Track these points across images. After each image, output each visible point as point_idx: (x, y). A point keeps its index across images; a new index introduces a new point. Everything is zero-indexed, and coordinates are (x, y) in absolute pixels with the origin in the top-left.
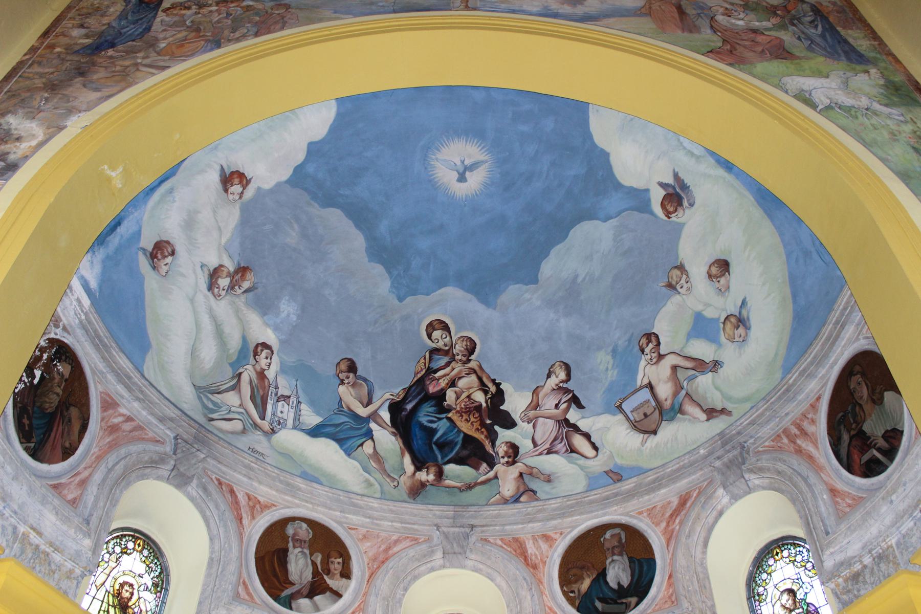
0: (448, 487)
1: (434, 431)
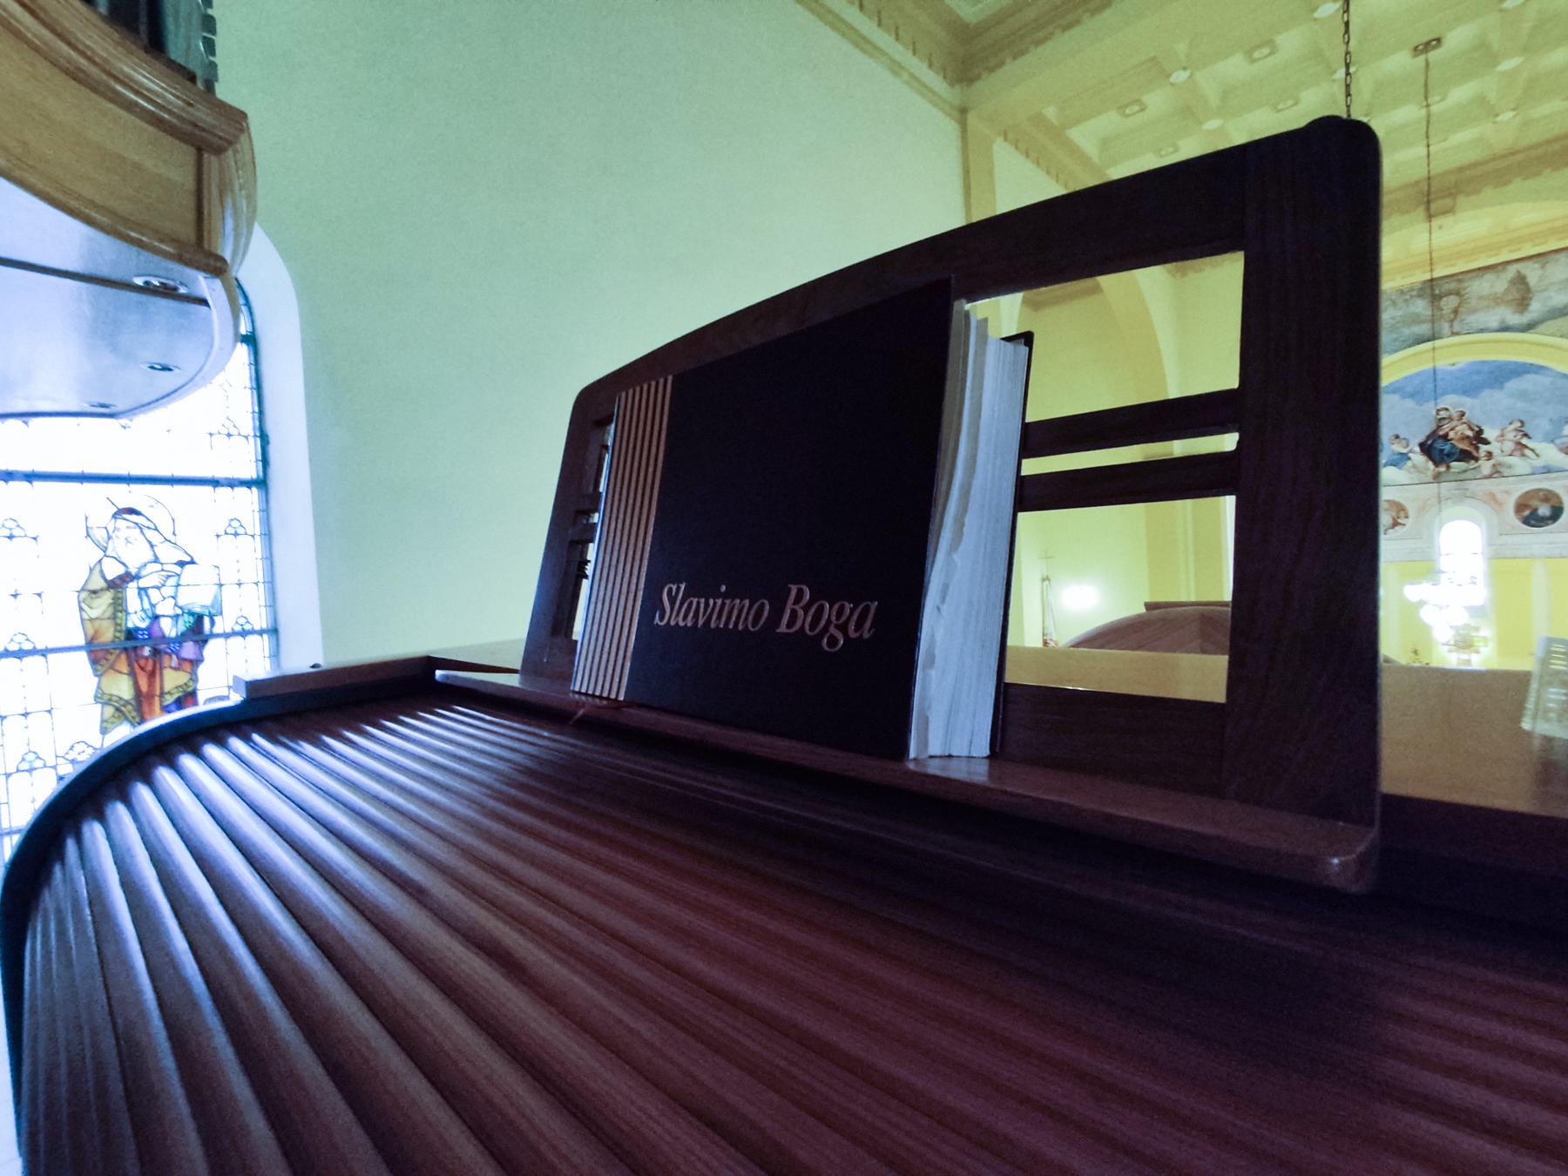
0: (1454, 472)
1: (1442, 451)
